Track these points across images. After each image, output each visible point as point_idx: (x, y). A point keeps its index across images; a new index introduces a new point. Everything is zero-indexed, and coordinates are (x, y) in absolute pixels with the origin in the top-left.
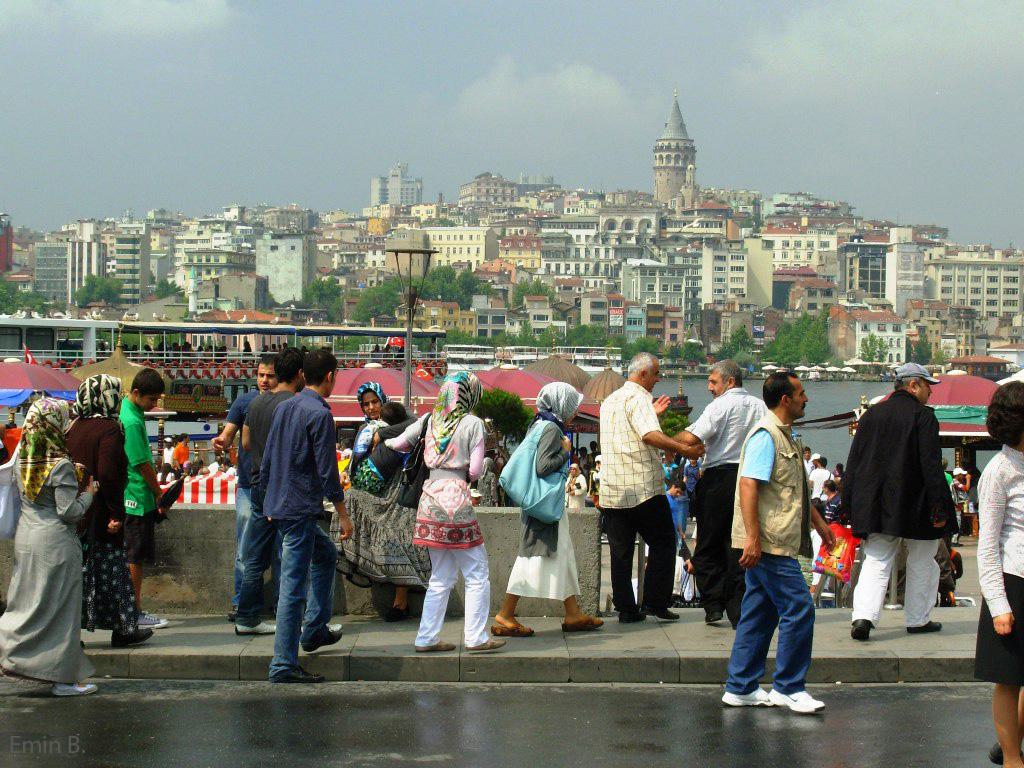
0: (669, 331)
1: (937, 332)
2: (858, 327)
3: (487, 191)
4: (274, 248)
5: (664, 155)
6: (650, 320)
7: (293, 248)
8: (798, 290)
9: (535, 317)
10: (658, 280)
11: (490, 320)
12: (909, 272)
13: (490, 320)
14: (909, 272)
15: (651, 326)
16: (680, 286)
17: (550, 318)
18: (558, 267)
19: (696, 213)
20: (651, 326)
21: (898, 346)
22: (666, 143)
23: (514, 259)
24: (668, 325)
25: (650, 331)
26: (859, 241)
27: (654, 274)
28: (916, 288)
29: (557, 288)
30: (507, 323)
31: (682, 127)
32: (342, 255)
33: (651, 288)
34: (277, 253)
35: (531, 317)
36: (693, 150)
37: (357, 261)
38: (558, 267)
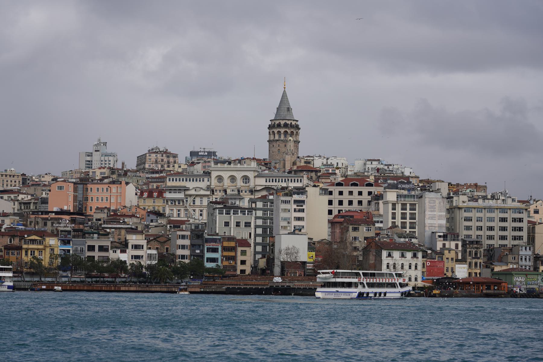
0: (240, 258)
1: (452, 259)
2: (384, 253)
3: (156, 161)
5: (276, 131)
8: (345, 226)
9: (132, 246)
10: (232, 217)
11: (97, 248)
12: (435, 213)
13: (97, 248)
14: (435, 213)
16: (250, 223)
17: (145, 247)
19: (293, 172)
22: (277, 122)
23: (149, 206)
24: (239, 253)
27: (230, 214)
28: (440, 226)
29: (168, 226)
30: (111, 251)
31: (289, 109)
32: (20, 203)
33: (227, 224)
35: (130, 246)
36: (297, 127)
37: (32, 208)
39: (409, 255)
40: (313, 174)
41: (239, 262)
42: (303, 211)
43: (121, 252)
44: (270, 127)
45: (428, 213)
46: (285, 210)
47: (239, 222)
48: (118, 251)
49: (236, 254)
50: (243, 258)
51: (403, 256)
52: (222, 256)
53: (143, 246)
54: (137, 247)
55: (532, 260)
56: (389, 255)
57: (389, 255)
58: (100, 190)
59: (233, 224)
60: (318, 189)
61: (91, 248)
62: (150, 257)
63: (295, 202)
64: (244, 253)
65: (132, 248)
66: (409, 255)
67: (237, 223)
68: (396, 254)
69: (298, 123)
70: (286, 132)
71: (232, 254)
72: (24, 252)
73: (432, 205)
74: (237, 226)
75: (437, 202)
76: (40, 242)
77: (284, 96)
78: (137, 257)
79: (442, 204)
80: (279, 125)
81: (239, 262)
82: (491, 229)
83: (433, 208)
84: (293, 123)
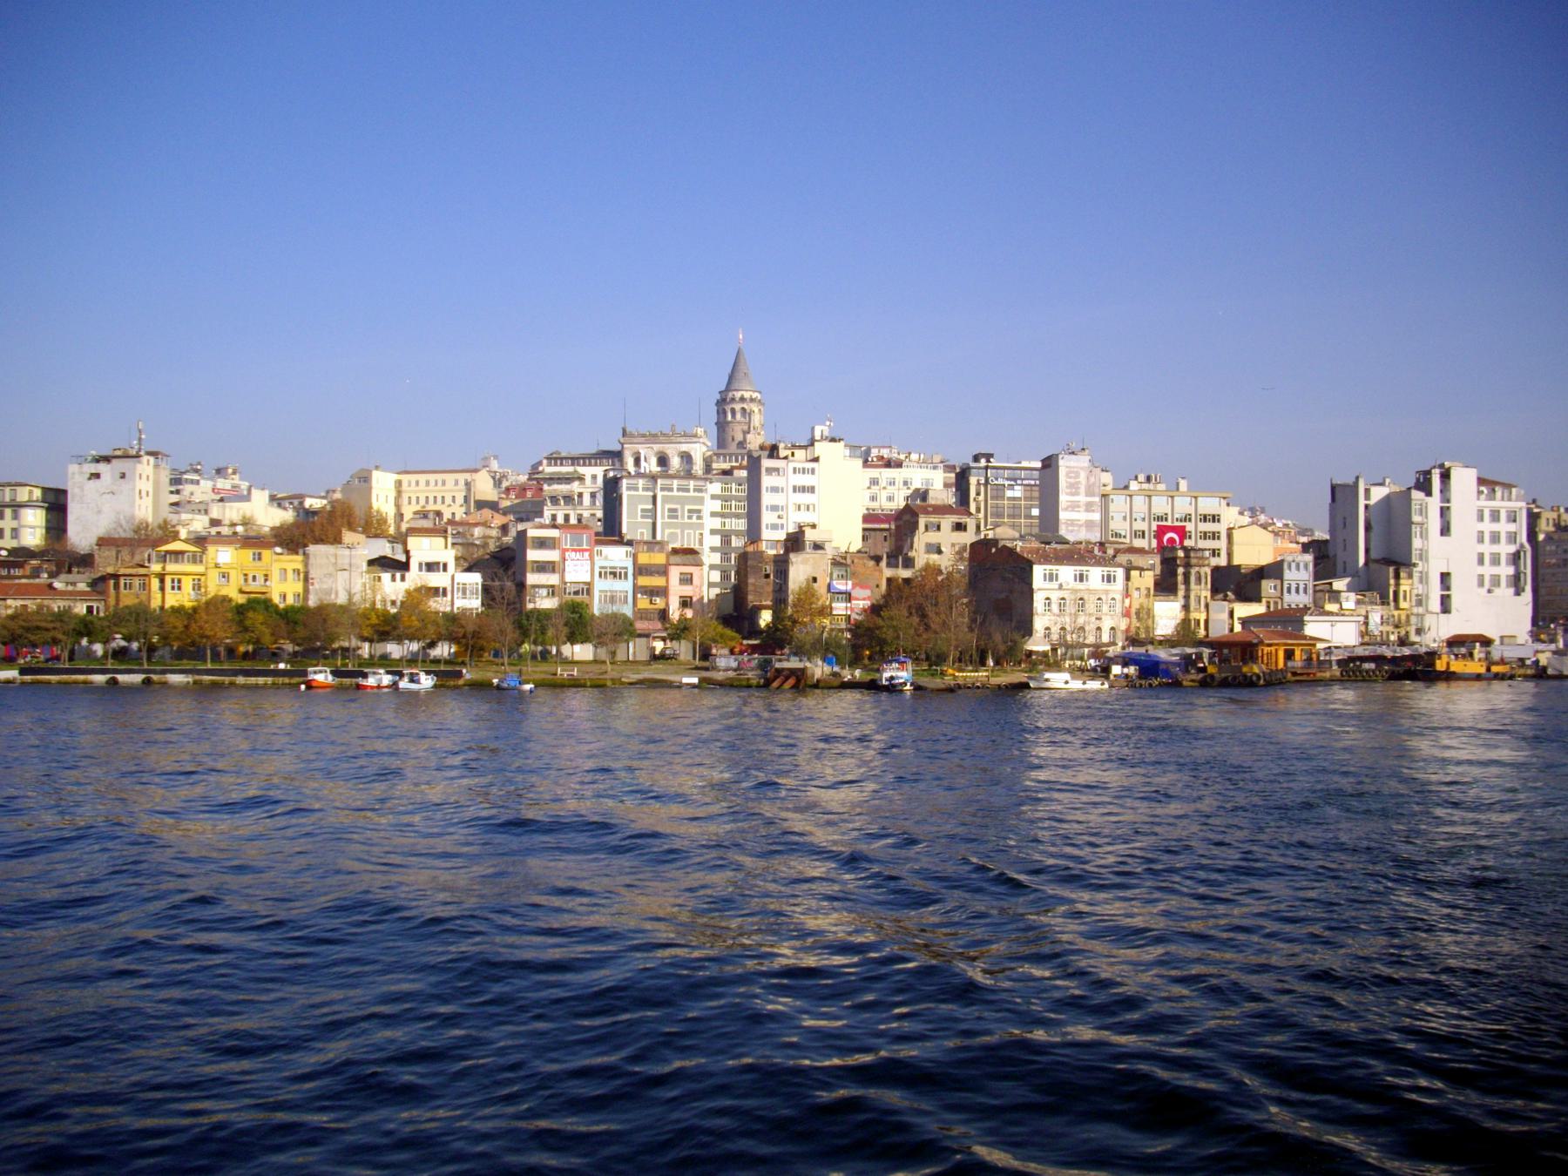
0: (677, 590)
2: (1038, 571)
4: (97, 476)
6: (640, 570)
9: (420, 564)
15: (644, 581)
18: (567, 517)
20: (644, 581)
26: (988, 461)
28: (1089, 525)
34: (94, 483)
38: (567, 517)
42: (812, 490)
45: (1064, 499)
46: (775, 490)
47: (675, 510)
49: (667, 581)
52: (635, 585)
53: (445, 566)
54: (431, 567)
56: (1051, 577)
58: (432, 483)
64: (687, 580)
65: (420, 570)
67: (670, 510)
71: (657, 581)
73: (1072, 481)
76: (194, 556)
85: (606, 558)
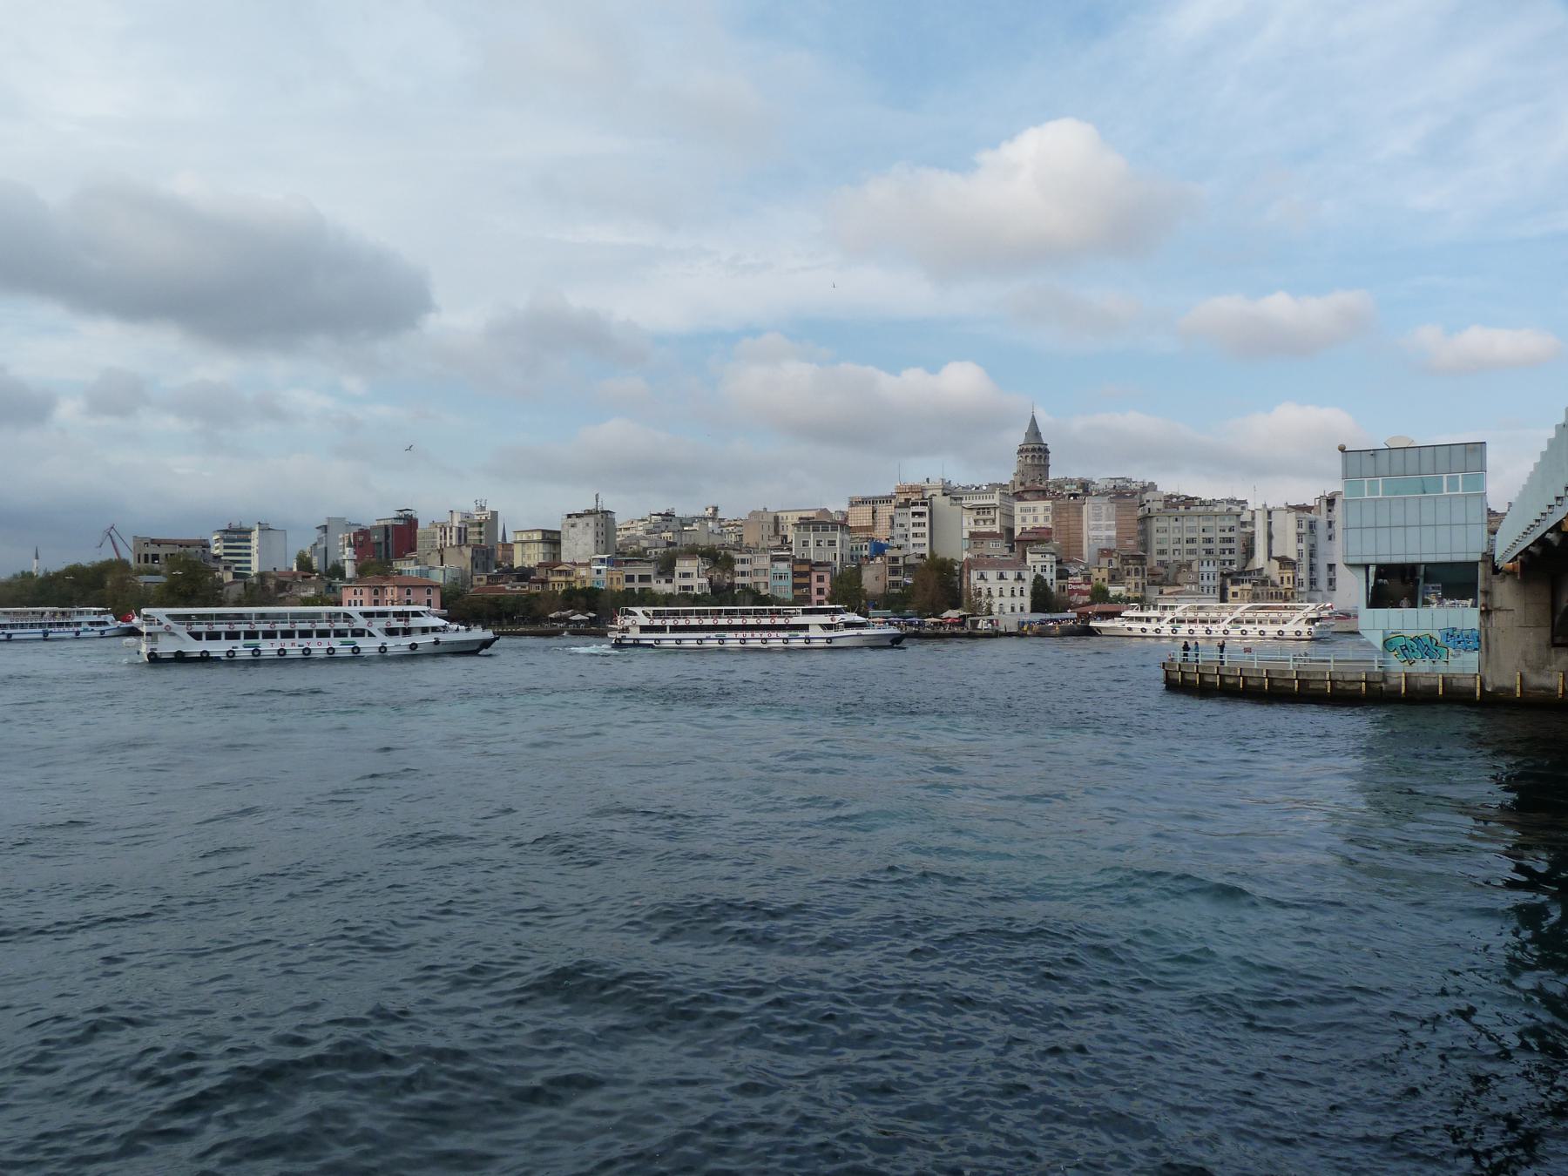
0: (815, 585)
5: (1024, 455)
6: (796, 574)
7: (587, 525)
11: (637, 578)
13: (637, 578)
15: (798, 580)
16: (835, 541)
17: (695, 575)
20: (798, 580)
21: (1022, 594)
25: (795, 586)
28: (1109, 539)
30: (654, 581)
33: (805, 544)
36: (1047, 451)
39: (1011, 575)
40: (1041, 493)
41: (814, 591)
43: (667, 581)
44: (1020, 451)
48: (663, 581)
50: (821, 585)
51: (1001, 577)
54: (686, 575)
55: (1218, 578)
56: (982, 577)
57: (982, 577)
59: (811, 544)
60: (948, 498)
61: (630, 579)
62: (701, 586)
63: (914, 514)
64: (820, 579)
66: (1011, 575)
68: (992, 575)
69: (1048, 447)
70: (1033, 456)
71: (805, 580)
72: (551, 585)
74: (818, 545)
75: (1104, 508)
77: (1033, 417)
78: (686, 588)
79: (1110, 510)
80: (1027, 450)
81: (814, 591)
82: (1192, 541)
83: (1097, 517)
84: (1042, 447)
85: (777, 569)
